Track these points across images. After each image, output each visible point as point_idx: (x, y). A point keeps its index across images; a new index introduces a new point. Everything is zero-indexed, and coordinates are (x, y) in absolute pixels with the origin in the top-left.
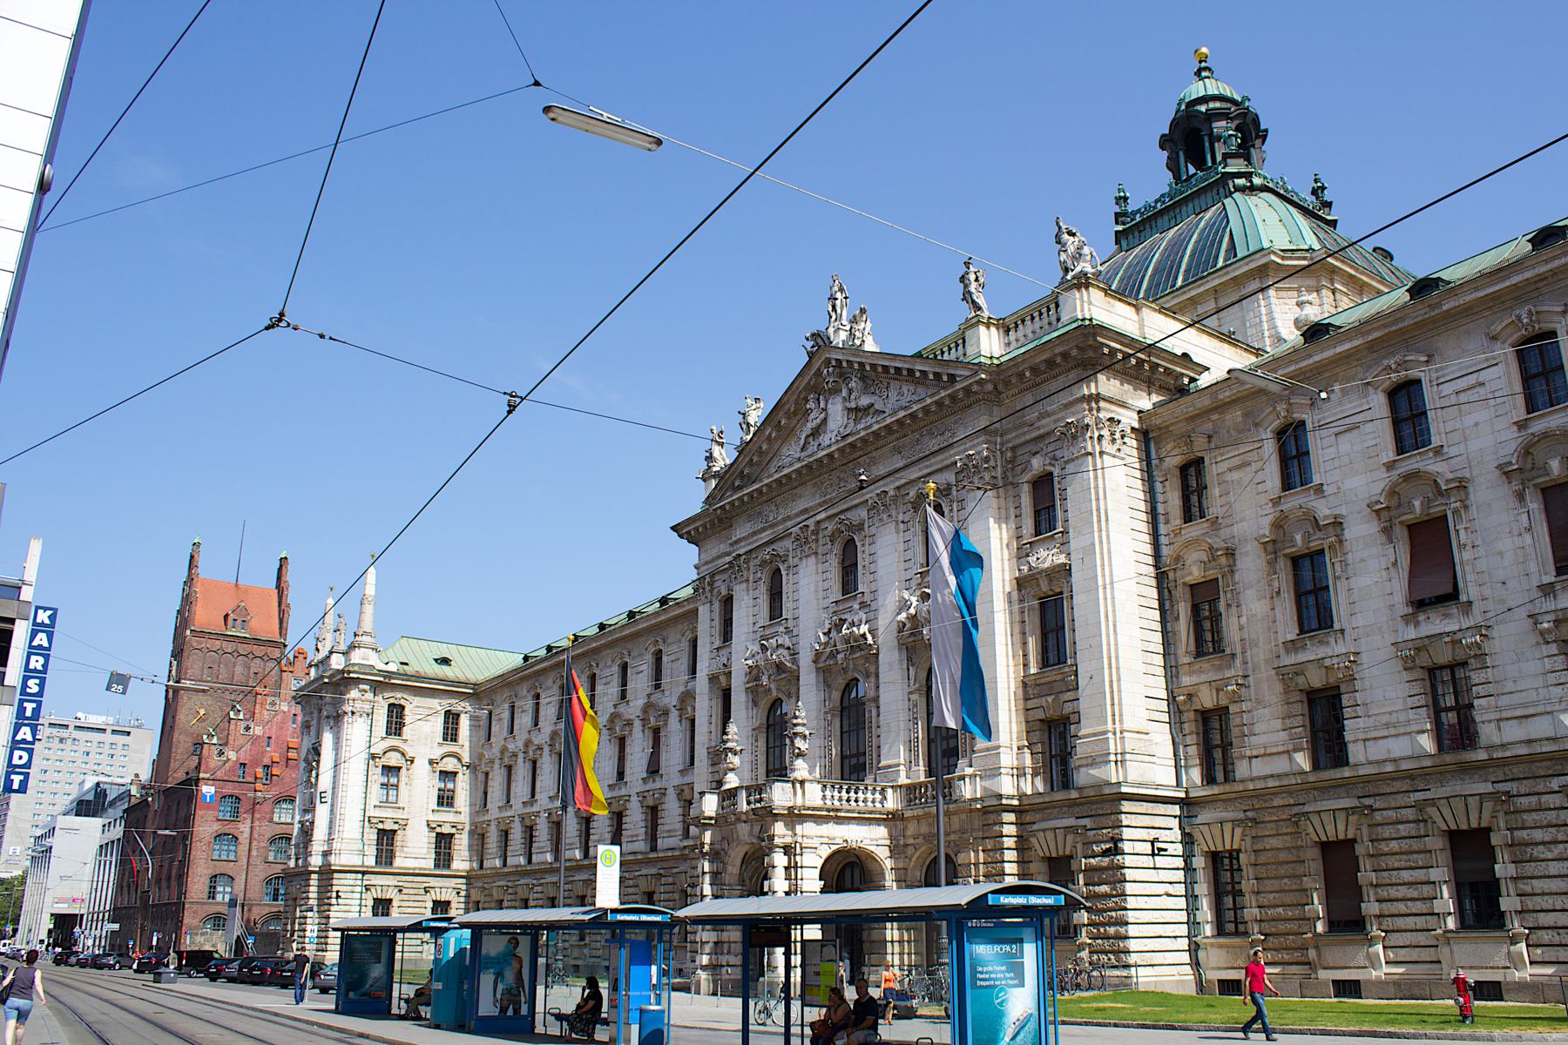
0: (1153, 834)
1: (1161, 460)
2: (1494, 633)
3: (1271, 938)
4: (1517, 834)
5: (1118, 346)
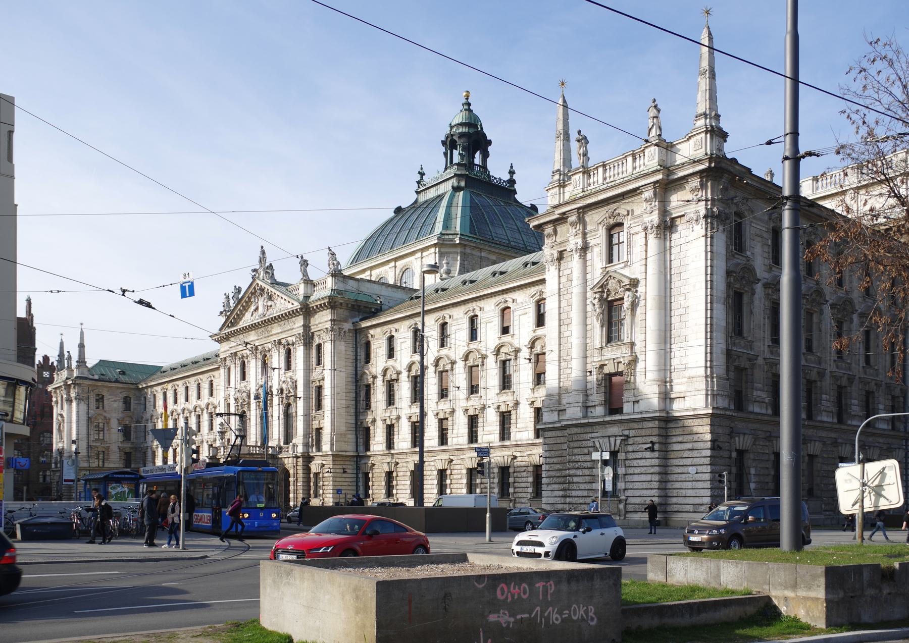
0: (344, 467)
1: (360, 340)
5: (342, 302)
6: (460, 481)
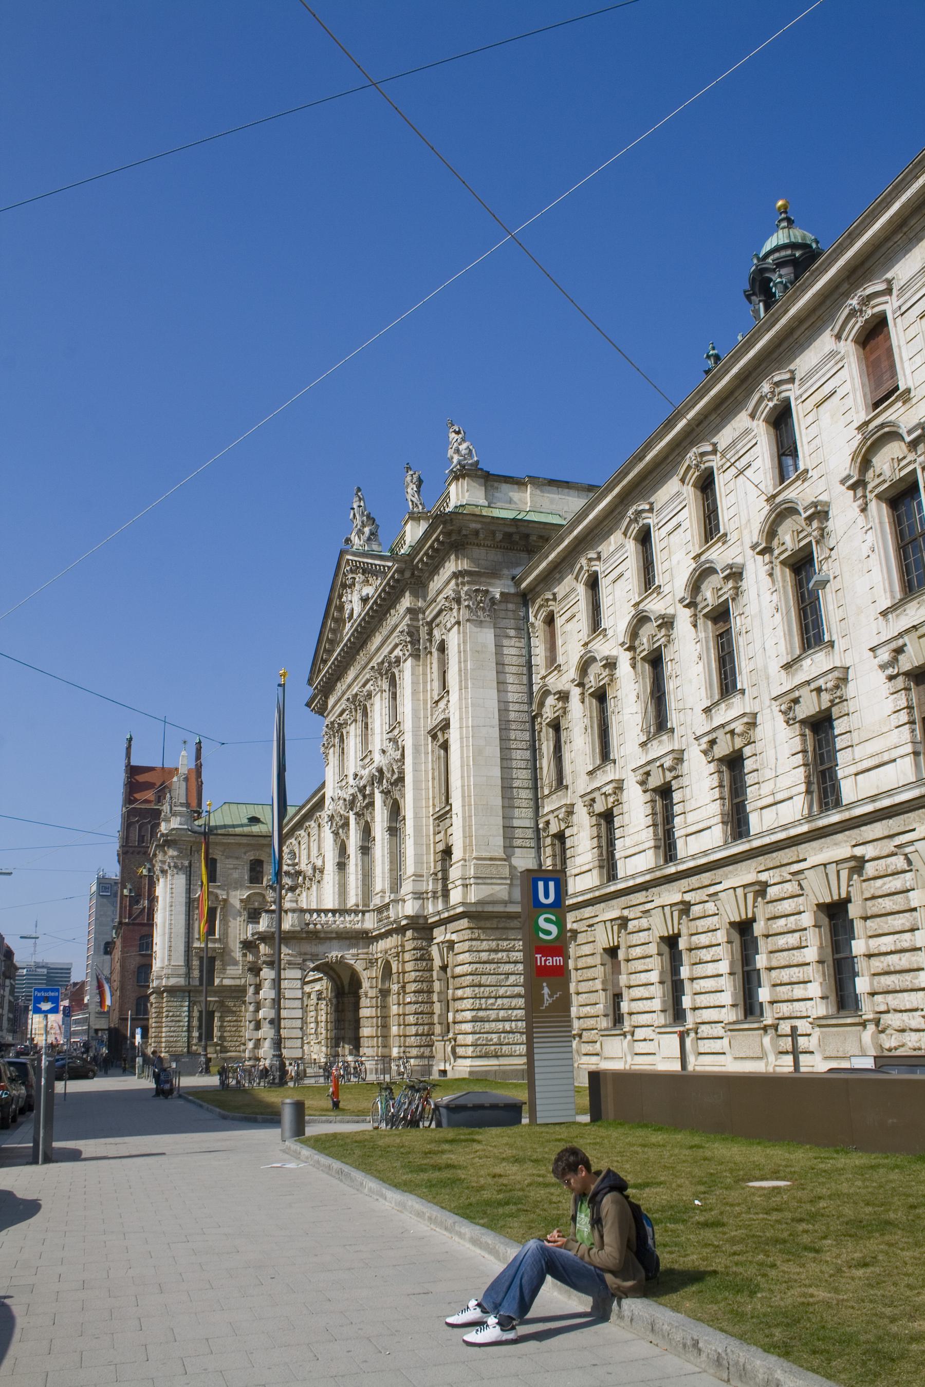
2: (686, 757)
3: (585, 1033)
4: (694, 938)
5: (479, 526)
6: (797, 956)
